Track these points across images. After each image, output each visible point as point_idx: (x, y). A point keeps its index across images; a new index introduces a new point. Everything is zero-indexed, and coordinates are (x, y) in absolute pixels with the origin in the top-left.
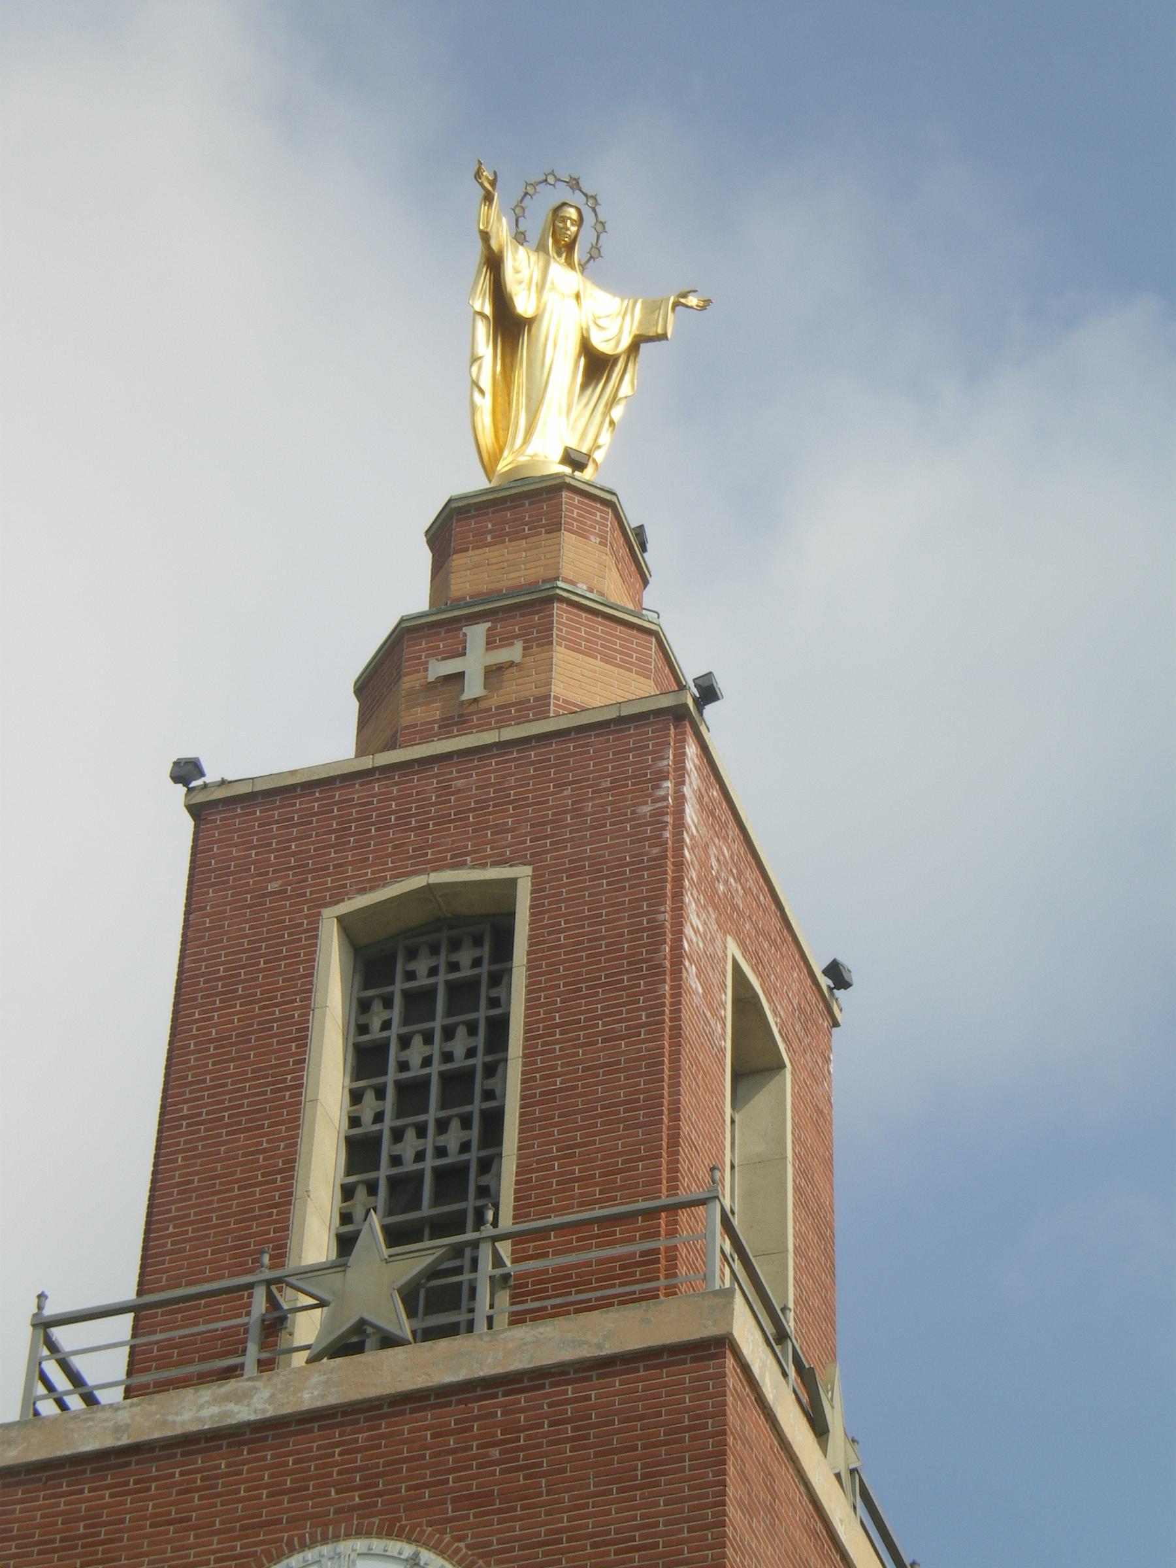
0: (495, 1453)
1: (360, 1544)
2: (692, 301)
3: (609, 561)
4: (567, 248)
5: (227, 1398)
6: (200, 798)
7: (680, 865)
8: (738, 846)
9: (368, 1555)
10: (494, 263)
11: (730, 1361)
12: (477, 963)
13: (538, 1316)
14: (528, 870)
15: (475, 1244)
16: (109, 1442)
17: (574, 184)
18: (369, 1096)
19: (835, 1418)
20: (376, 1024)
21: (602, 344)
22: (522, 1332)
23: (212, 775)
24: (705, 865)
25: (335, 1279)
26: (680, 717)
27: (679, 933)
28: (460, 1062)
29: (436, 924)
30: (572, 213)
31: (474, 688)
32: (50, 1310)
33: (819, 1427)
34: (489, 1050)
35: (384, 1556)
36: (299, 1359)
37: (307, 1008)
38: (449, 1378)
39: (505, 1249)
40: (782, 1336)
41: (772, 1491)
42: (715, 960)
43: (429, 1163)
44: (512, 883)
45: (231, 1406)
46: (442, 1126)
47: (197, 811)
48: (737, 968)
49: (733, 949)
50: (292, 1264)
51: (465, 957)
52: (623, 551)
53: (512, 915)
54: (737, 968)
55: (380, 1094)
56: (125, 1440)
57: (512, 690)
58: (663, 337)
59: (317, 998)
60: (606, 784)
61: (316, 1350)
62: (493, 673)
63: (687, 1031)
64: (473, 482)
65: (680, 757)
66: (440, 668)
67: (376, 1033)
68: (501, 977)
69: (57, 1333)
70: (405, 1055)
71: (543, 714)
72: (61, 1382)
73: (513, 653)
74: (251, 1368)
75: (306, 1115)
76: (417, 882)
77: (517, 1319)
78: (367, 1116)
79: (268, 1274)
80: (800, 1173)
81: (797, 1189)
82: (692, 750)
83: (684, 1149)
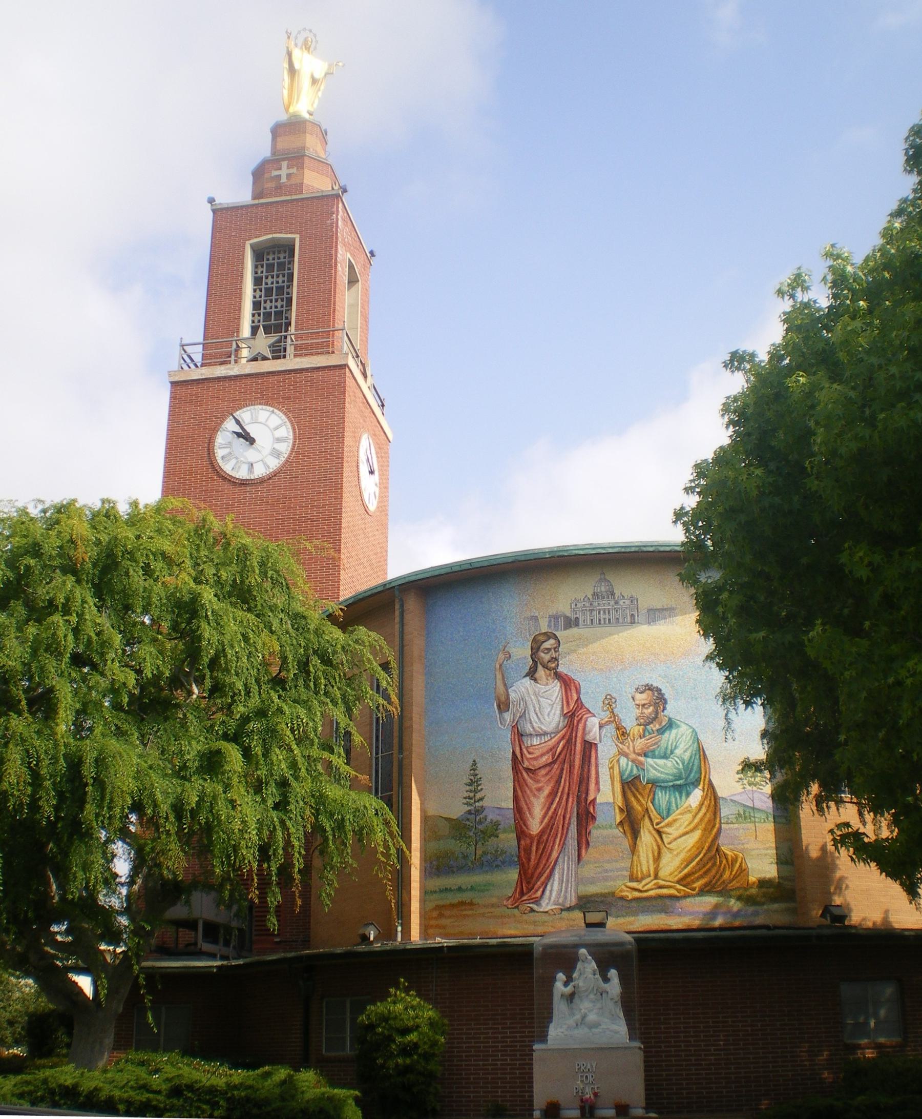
0: (292, 387)
1: (260, 407)
2: (340, 64)
3: (318, 142)
4: (308, 49)
5: (227, 369)
6: (214, 208)
7: (337, 238)
8: (351, 227)
9: (262, 409)
10: (289, 54)
11: (347, 369)
12: (285, 258)
13: (301, 355)
14: (298, 236)
15: (286, 337)
16: (200, 377)
17: (310, 31)
18: (258, 291)
19: (369, 373)
20: (259, 272)
21: (317, 76)
22: (298, 359)
23: (217, 202)
24: (343, 235)
25: (252, 341)
26: (338, 196)
27: (336, 256)
28: (281, 284)
29: (274, 247)
30: (310, 39)
31: (284, 180)
32: (184, 342)
33: (365, 375)
34: (288, 282)
35: (266, 410)
36: (244, 361)
37: (243, 268)
38: (280, 369)
39: (293, 337)
40: (358, 356)
41: (355, 397)
42: (344, 260)
43: (273, 310)
44: (294, 239)
45: (229, 371)
46: (276, 301)
47: (214, 211)
48: (349, 260)
49: (349, 255)
50: (241, 337)
51: (282, 256)
52: (322, 138)
53: (294, 245)
54: (349, 260)
55: (261, 291)
56: (203, 377)
57: (294, 181)
58: (333, 73)
59: (245, 266)
60: (318, 214)
61: (249, 358)
62: (289, 176)
63: (338, 282)
64: (283, 117)
65: (338, 207)
66: (275, 173)
67: (259, 274)
68: (291, 262)
69: (185, 347)
70: (267, 281)
71: (301, 192)
72: (188, 360)
73: (294, 170)
74: (233, 362)
75: (243, 296)
76: (270, 236)
77: (295, 356)
78: (258, 296)
79: (236, 338)
80: (362, 307)
81: (361, 312)
82: (340, 205)
83: (337, 313)
